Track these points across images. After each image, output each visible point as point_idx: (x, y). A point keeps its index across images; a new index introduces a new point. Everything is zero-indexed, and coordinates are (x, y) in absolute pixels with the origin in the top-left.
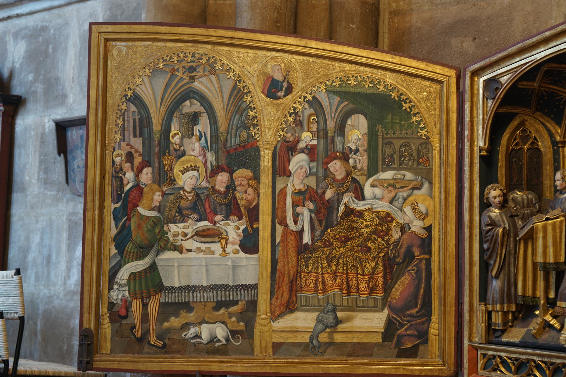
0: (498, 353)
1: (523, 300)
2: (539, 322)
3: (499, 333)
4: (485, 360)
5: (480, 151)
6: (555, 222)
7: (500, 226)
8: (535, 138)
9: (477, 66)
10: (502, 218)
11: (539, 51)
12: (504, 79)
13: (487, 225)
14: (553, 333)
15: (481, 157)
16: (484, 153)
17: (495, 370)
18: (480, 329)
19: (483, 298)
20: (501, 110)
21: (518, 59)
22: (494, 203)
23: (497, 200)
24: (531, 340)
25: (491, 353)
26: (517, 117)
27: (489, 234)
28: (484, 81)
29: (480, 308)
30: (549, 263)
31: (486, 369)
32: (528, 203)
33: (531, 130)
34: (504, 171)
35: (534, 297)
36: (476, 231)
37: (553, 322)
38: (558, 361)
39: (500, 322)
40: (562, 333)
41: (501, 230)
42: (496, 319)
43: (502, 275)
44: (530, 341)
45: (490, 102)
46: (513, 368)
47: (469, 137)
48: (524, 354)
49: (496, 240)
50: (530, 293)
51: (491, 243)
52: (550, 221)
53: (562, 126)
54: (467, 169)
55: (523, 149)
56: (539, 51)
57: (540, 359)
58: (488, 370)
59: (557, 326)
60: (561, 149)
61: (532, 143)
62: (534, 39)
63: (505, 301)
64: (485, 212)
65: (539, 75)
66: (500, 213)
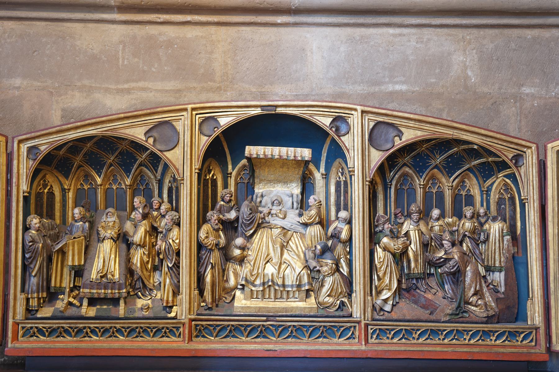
0: (36, 325)
1: (55, 290)
2: (65, 303)
3: (35, 312)
4: (24, 330)
5: (23, 193)
6: (79, 240)
7: (38, 243)
8: (51, 186)
9: (24, 137)
10: (39, 237)
11: (71, 133)
12: (42, 148)
13: (30, 242)
14: (74, 309)
15: (25, 197)
16: (26, 194)
17: (32, 336)
18: (21, 311)
19: (23, 290)
20: (38, 167)
21: (55, 136)
22: (34, 227)
23: (37, 225)
24: (60, 314)
25: (30, 325)
26: (42, 171)
27: (31, 248)
28: (28, 147)
29: (21, 297)
30: (75, 265)
31: (26, 336)
32: (52, 228)
33: (49, 180)
34: (34, 206)
35: (60, 287)
36: (20, 246)
37: (75, 302)
38: (81, 326)
39: (36, 304)
40: (83, 308)
41: (41, 245)
42: (32, 304)
43: (38, 274)
44: (59, 315)
45: (31, 162)
46: (47, 334)
47: (17, 183)
48: (55, 324)
49: (37, 252)
50: (58, 285)
51: (32, 253)
52: (76, 239)
53: (69, 179)
54: (14, 204)
55: (43, 192)
56: (71, 133)
57: (68, 325)
58: (27, 337)
59: (78, 304)
60: (67, 193)
61: (49, 189)
62: (69, 126)
63: (40, 291)
64: (26, 234)
65: (65, 148)
66: (38, 234)
